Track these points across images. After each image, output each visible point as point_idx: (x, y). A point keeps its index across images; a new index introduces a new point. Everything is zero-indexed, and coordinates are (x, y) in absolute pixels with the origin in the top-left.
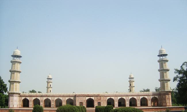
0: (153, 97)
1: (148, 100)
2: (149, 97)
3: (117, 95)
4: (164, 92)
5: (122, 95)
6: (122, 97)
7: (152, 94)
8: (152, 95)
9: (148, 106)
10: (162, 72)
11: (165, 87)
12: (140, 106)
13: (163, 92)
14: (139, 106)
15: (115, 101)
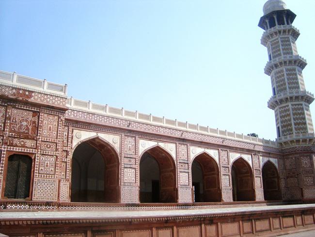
0: (266, 159)
1: (255, 172)
2: (255, 158)
3: (133, 127)
4: (304, 145)
5: (162, 132)
6: (162, 145)
7: (261, 149)
8: (266, 154)
9: (257, 200)
10: (290, 70)
11: (305, 124)
12: (232, 201)
13: (298, 141)
14: (129, 206)
15: (124, 162)
